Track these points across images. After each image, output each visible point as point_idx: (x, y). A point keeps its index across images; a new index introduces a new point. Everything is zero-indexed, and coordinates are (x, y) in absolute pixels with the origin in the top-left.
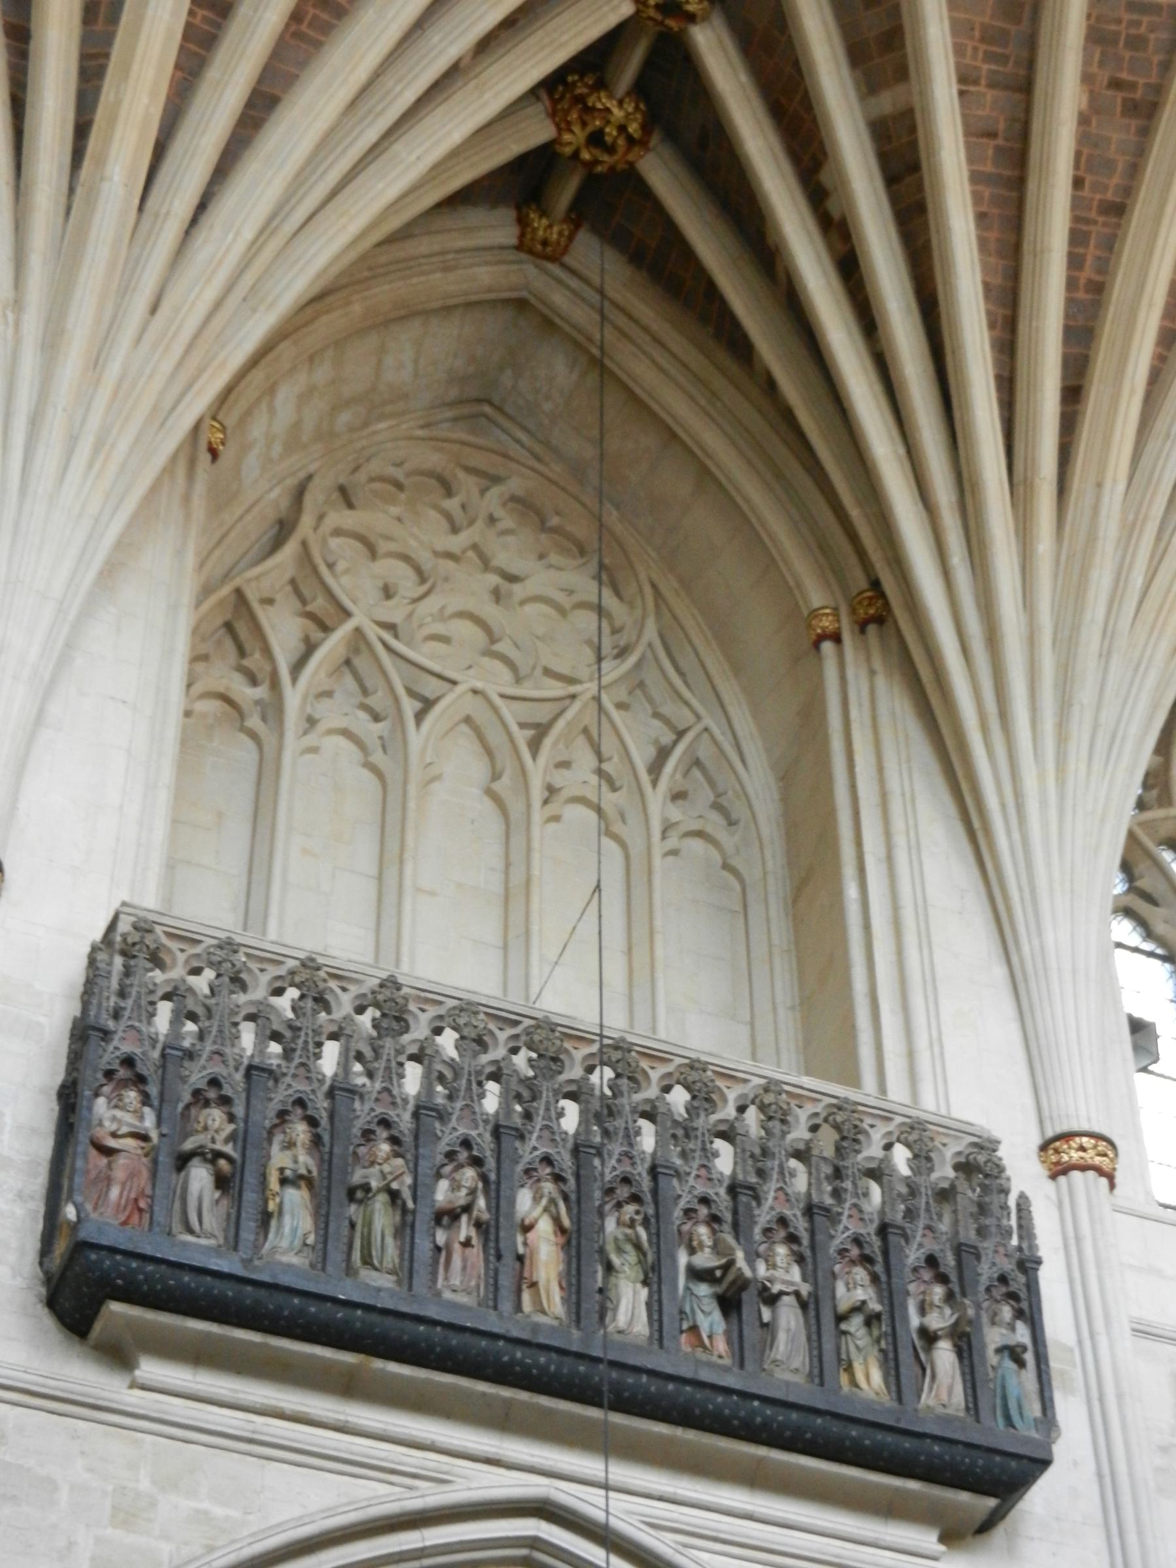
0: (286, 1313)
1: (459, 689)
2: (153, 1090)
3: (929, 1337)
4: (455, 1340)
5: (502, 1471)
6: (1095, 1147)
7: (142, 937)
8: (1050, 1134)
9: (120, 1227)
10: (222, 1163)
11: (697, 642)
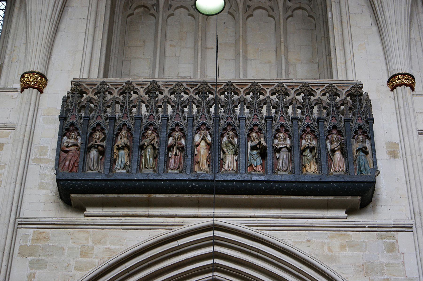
0: (121, 187)
3: (333, 151)
5: (199, 219)
6: (404, 77)
7: (76, 88)
9: (69, 173)
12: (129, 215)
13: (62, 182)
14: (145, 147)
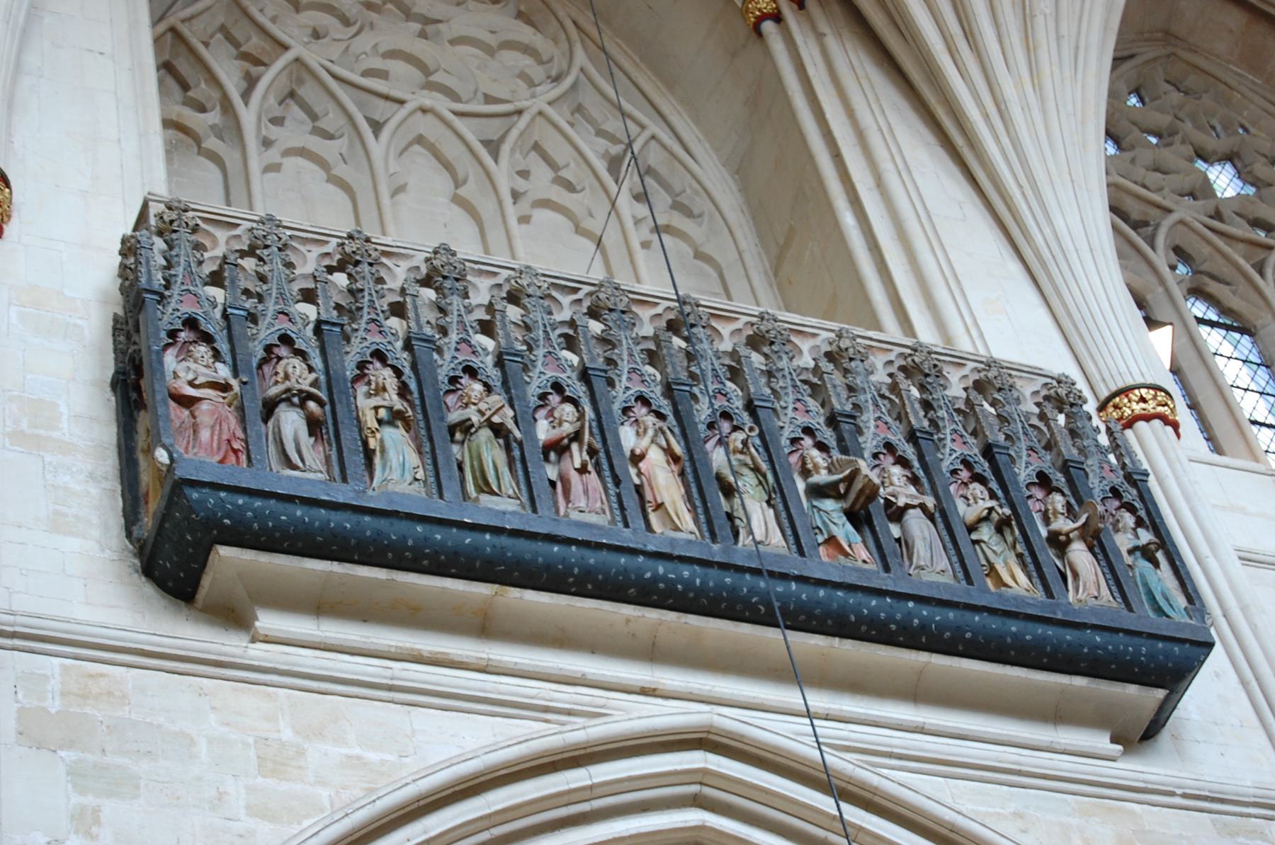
0: (410, 543)
1: (409, 107)
2: (224, 347)
3: (1059, 543)
4: (592, 558)
5: (659, 701)
6: (1155, 397)
8: (1104, 394)
10: (312, 405)
11: (627, 65)
12: (422, 656)
13: (198, 492)
14: (473, 430)
